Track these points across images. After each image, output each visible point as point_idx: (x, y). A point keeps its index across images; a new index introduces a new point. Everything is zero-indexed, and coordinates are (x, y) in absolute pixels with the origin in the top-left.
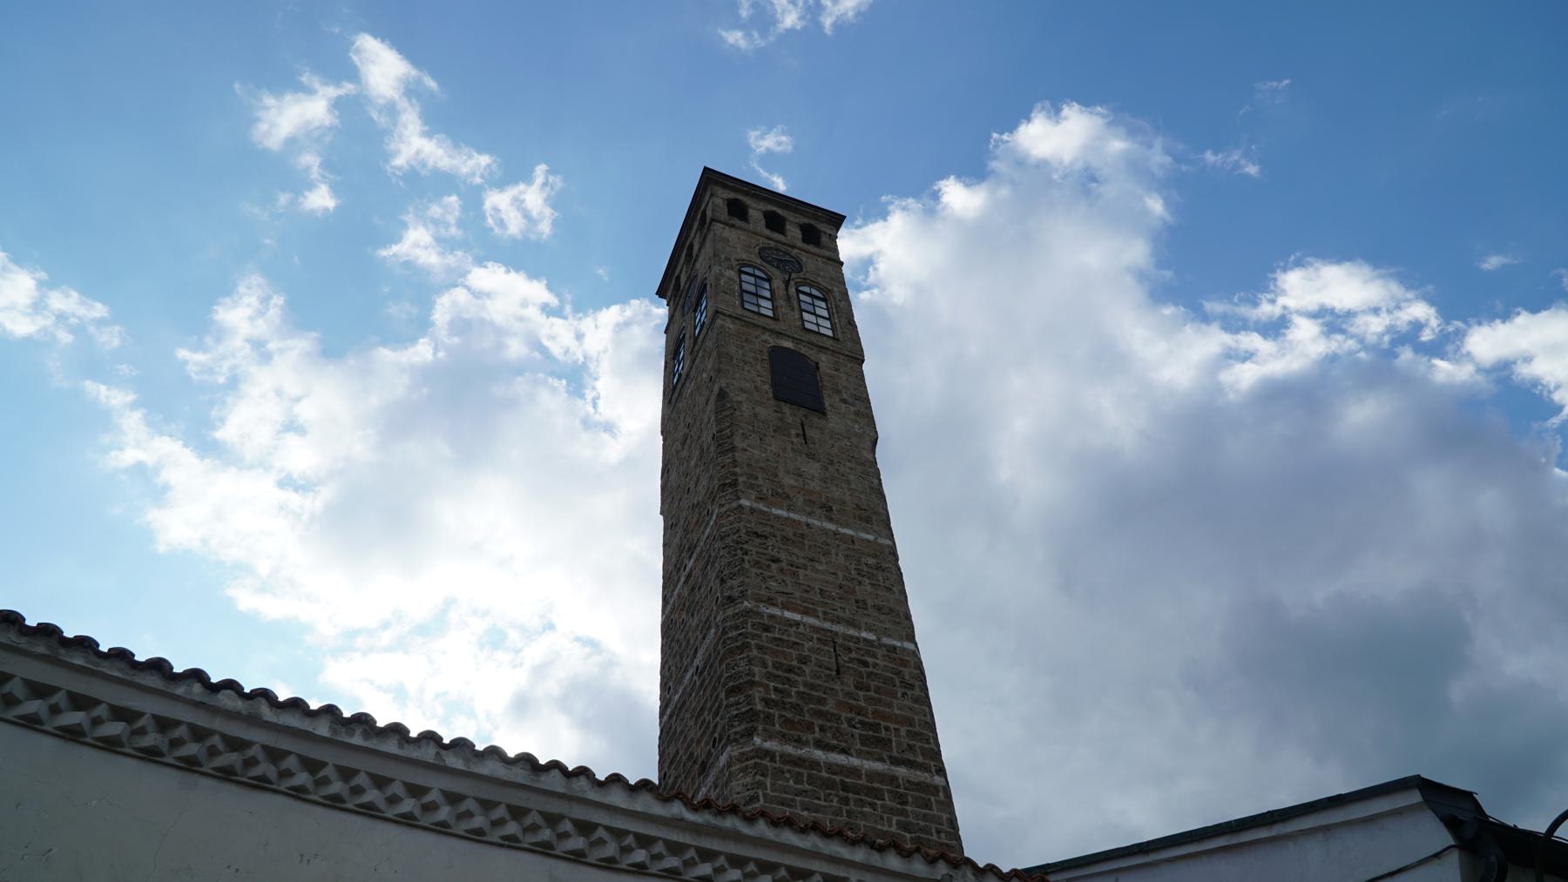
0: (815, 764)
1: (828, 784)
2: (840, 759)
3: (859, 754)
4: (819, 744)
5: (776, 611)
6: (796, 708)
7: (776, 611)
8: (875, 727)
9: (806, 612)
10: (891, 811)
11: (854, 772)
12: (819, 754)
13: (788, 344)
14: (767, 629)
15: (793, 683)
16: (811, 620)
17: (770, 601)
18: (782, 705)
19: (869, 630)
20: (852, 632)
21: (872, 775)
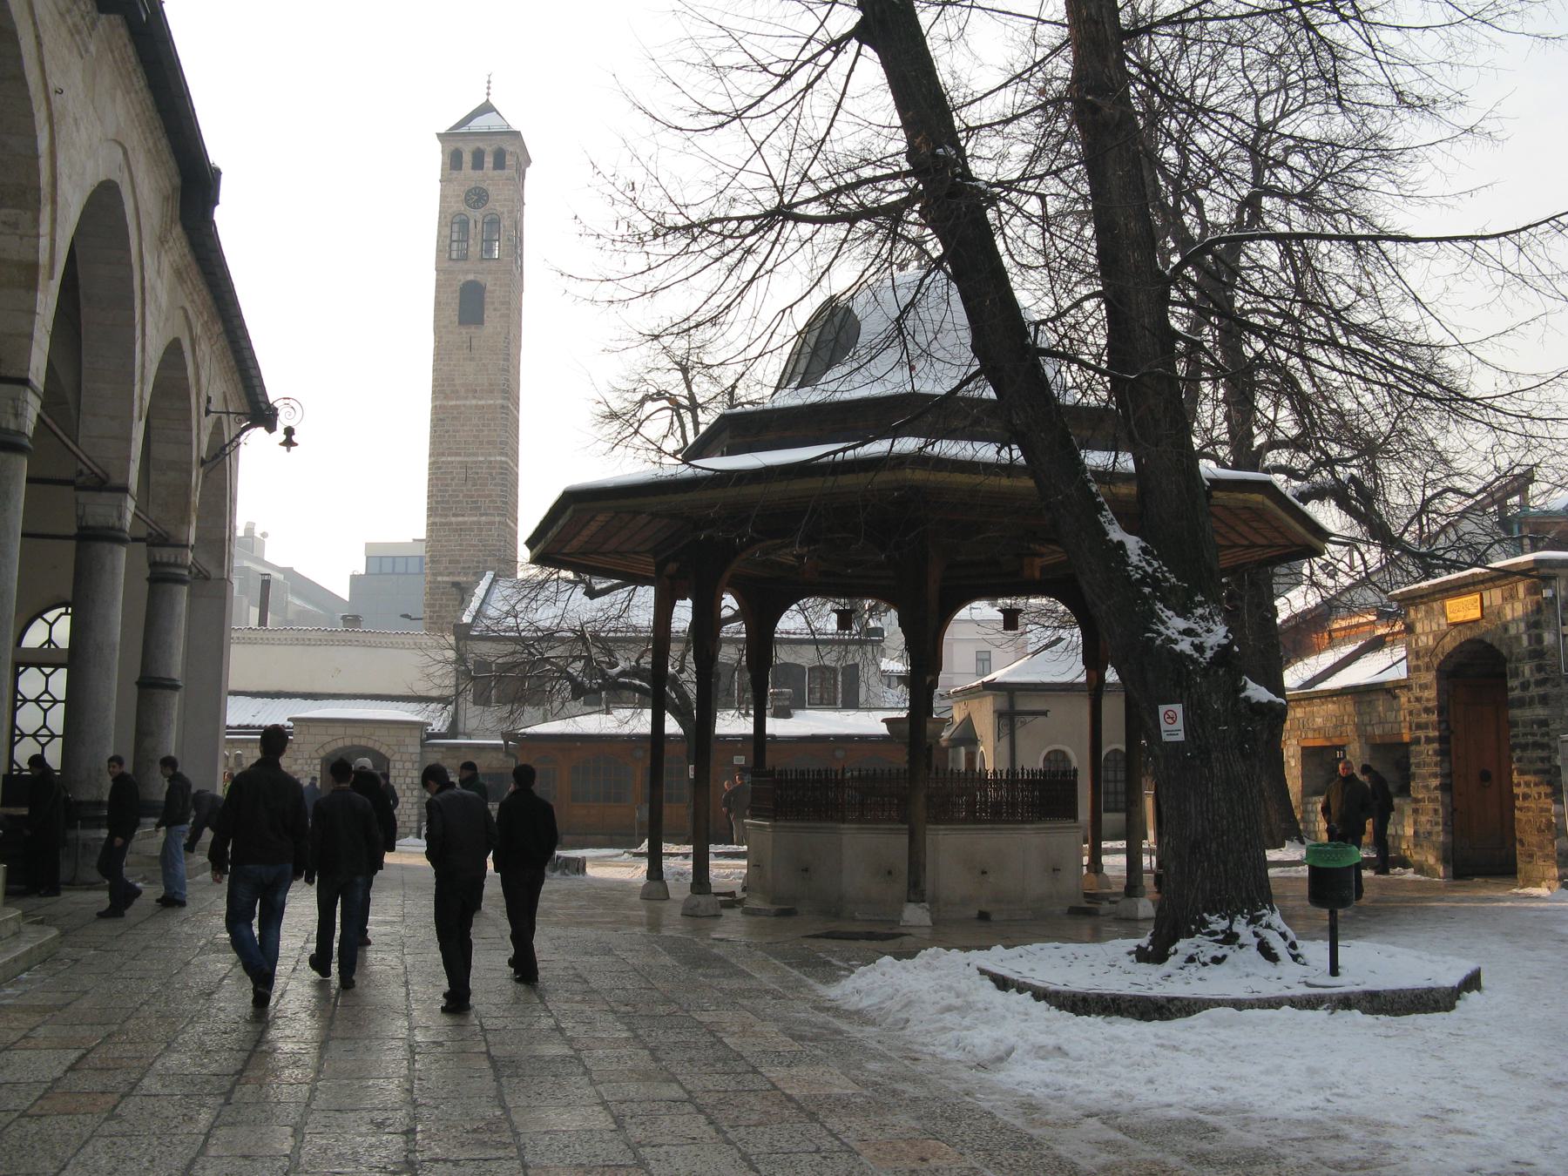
0: (451, 524)
1: (456, 530)
2: (460, 519)
3: (470, 515)
4: (454, 515)
5: (444, 459)
6: (448, 502)
7: (444, 459)
8: (476, 502)
9: (458, 454)
10: (475, 536)
11: (465, 523)
12: (453, 519)
13: (471, 277)
14: (440, 468)
15: (446, 491)
16: (458, 459)
17: (443, 454)
18: (443, 502)
19: (482, 455)
20: (475, 459)
21: (473, 523)
